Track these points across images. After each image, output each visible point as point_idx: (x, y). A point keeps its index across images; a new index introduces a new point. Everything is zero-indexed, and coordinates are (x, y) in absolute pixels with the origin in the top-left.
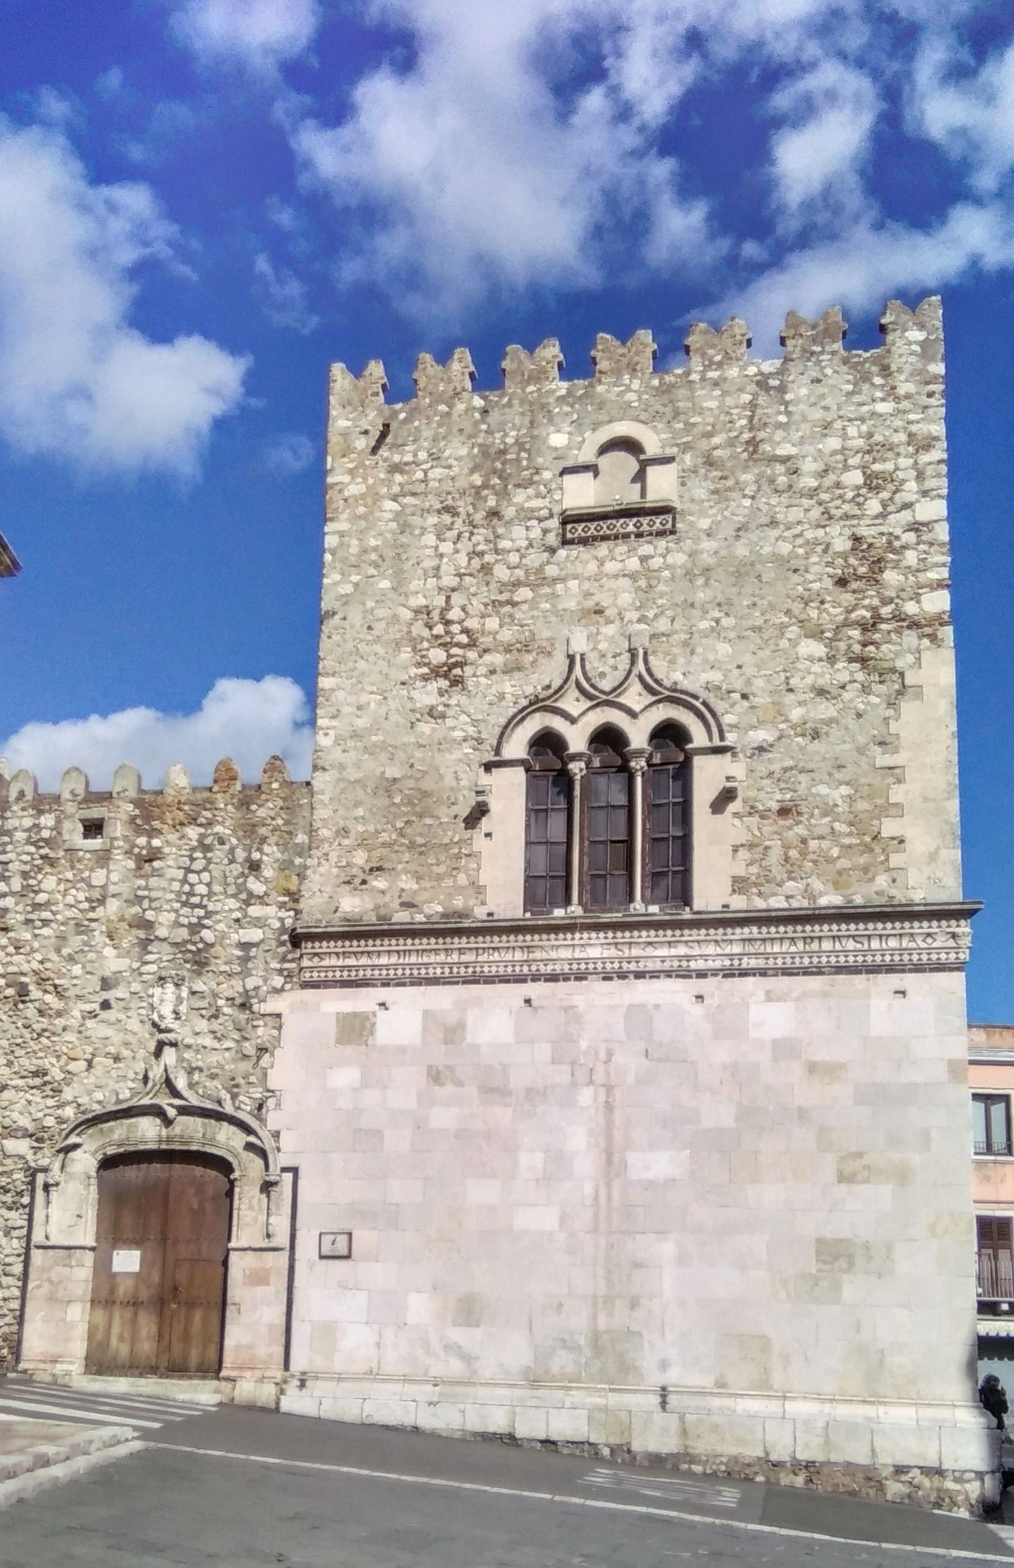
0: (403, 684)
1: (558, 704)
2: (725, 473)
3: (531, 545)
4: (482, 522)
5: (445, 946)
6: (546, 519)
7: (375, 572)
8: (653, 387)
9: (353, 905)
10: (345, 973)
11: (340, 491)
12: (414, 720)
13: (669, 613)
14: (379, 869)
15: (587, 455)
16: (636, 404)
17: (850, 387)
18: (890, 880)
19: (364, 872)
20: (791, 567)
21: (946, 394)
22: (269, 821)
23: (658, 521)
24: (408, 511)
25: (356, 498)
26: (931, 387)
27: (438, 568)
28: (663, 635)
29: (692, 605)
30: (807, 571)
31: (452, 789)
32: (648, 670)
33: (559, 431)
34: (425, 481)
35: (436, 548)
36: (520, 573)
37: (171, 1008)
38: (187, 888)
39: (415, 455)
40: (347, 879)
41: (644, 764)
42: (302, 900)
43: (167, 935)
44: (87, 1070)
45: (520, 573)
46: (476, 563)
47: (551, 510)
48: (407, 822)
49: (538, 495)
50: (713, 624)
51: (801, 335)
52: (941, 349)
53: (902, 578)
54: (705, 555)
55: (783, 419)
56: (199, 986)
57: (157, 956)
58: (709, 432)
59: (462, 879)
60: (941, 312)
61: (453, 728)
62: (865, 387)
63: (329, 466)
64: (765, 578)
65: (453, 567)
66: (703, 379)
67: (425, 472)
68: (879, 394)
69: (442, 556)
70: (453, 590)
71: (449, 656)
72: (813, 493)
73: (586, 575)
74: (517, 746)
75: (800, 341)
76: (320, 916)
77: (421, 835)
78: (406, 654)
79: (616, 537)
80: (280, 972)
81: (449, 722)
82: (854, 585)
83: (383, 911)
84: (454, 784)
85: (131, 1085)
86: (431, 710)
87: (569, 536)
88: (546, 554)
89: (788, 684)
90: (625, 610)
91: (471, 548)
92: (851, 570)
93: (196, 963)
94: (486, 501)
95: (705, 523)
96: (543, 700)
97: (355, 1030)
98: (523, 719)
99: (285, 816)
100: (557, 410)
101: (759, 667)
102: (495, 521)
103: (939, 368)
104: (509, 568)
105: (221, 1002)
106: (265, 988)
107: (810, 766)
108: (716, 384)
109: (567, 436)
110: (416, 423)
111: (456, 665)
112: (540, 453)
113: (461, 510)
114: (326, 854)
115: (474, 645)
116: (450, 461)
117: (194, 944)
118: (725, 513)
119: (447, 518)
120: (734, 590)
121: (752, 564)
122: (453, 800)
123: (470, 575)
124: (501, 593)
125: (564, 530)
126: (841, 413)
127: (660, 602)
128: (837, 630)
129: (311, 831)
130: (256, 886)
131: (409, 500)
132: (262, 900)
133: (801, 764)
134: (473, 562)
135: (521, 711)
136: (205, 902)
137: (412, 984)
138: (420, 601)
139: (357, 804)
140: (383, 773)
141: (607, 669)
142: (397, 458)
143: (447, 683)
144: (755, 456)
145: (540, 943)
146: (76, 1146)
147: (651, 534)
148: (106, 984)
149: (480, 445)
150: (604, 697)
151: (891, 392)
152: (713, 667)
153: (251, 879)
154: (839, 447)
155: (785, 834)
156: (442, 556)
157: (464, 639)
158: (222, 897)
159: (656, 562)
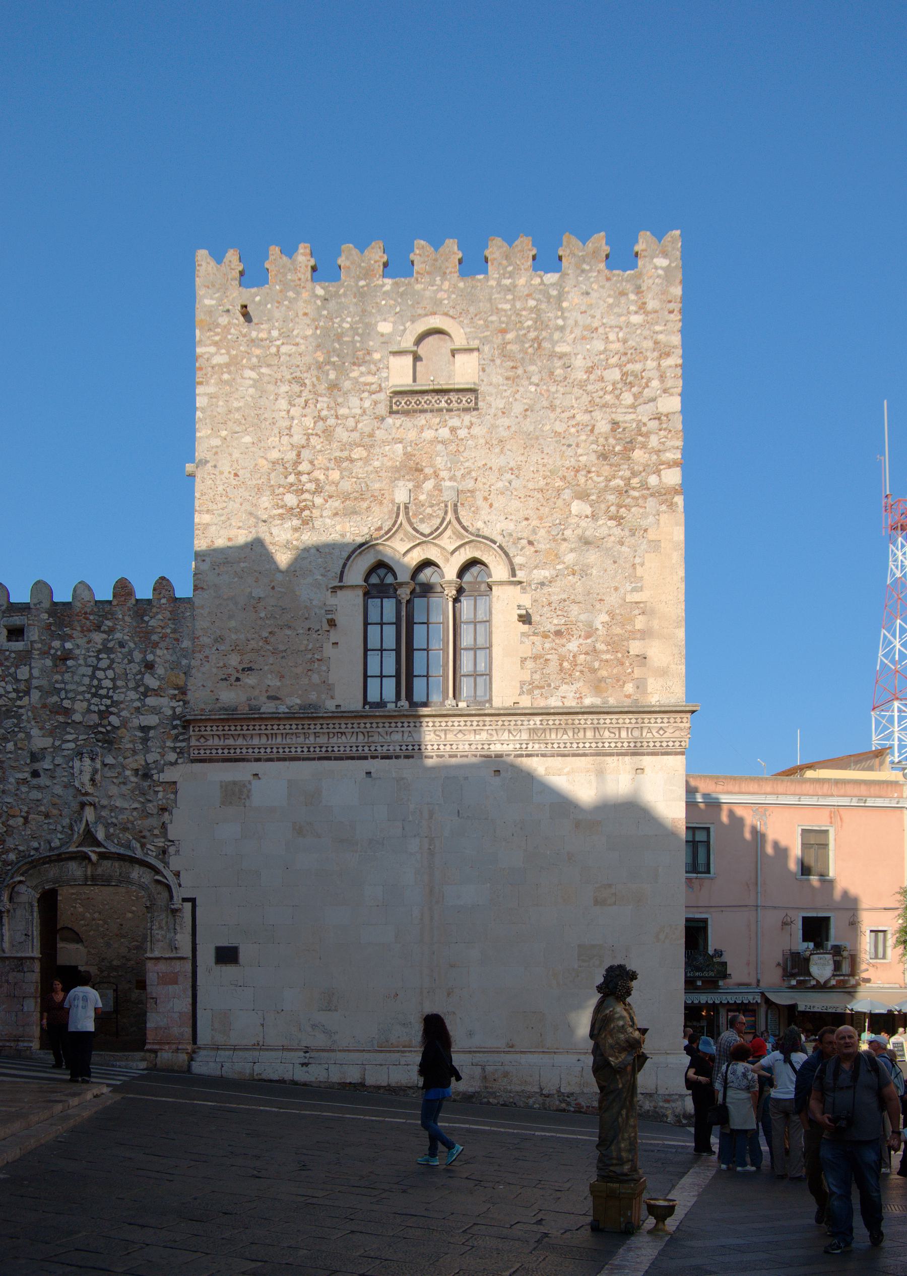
0: (265, 521)
4: (324, 392)
6: (379, 392)
7: (238, 429)
9: (229, 696)
11: (208, 360)
13: (474, 474)
14: (250, 669)
17: (611, 301)
19: (238, 671)
21: (681, 311)
22: (159, 630)
23: (464, 400)
24: (266, 379)
25: (220, 365)
26: (672, 306)
27: (290, 428)
29: (491, 468)
32: (458, 519)
33: (385, 320)
35: (288, 412)
36: (355, 435)
37: (88, 777)
38: (95, 682)
39: (270, 333)
40: (223, 677)
42: (189, 693)
43: (81, 719)
44: (25, 824)
45: (355, 435)
47: (380, 385)
48: (270, 633)
49: (369, 373)
50: (507, 484)
52: (679, 276)
55: (560, 322)
56: (110, 760)
57: (74, 736)
60: (680, 244)
62: (623, 300)
63: (197, 339)
67: (278, 348)
68: (633, 308)
69: (293, 418)
70: (303, 447)
72: (582, 385)
76: (203, 706)
78: (265, 501)
79: (432, 411)
80: (174, 749)
83: (253, 703)
85: (60, 836)
86: (287, 543)
87: (395, 408)
91: (316, 414)
93: (106, 741)
94: (328, 375)
98: (360, 553)
99: (173, 626)
100: (383, 302)
103: (677, 291)
105: (128, 773)
106: (162, 762)
108: (509, 289)
110: (269, 306)
113: (307, 381)
114: (207, 657)
116: (298, 340)
117: (104, 727)
119: (296, 388)
120: (523, 458)
123: (317, 435)
124: (342, 451)
126: (604, 321)
127: (466, 464)
129: (194, 639)
130: (151, 682)
131: (264, 370)
132: (157, 693)
136: (111, 694)
138: (274, 455)
139: (230, 617)
140: (251, 593)
142: (254, 334)
146: (20, 882)
147: (459, 410)
148: (35, 757)
150: (425, 539)
153: (147, 676)
154: (602, 348)
158: (124, 690)
159: (462, 433)
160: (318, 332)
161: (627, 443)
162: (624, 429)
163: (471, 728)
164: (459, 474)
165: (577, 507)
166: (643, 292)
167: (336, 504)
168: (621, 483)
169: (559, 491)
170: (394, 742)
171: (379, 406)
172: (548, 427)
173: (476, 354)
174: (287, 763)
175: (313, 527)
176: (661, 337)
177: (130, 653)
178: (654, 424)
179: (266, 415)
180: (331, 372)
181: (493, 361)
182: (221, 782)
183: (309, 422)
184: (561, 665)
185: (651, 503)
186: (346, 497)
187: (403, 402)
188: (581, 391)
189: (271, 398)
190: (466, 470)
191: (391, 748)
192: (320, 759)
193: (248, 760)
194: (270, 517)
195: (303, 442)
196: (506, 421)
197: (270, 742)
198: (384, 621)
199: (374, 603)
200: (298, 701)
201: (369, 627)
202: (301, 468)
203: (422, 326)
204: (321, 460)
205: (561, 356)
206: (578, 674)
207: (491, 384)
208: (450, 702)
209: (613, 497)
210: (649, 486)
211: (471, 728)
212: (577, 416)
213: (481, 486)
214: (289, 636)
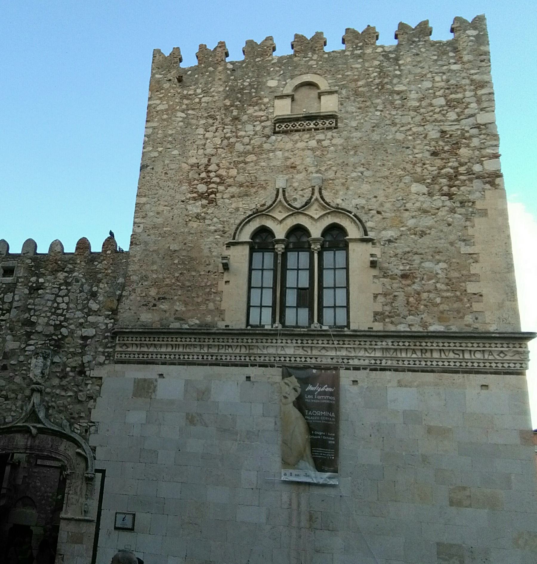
0: (183, 201)
1: (270, 214)
2: (365, 99)
3: (256, 134)
4: (229, 123)
5: (200, 343)
8: (325, 58)
10: (141, 356)
12: (188, 220)
14: (164, 298)
15: (288, 90)
16: (315, 66)
17: (436, 57)
18: (474, 318)
20: (403, 145)
28: (331, 180)
29: (347, 164)
30: (414, 148)
31: (208, 257)
32: (322, 198)
33: (272, 79)
34: (200, 103)
46: (225, 142)
47: (267, 117)
48: (181, 274)
50: (360, 174)
51: (407, 33)
53: (471, 152)
54: (354, 139)
55: (398, 73)
58: (356, 79)
59: (211, 306)
61: (209, 225)
64: (389, 151)
65: (212, 145)
66: (352, 54)
67: (200, 99)
69: (207, 139)
70: (213, 155)
71: (209, 189)
72: (416, 109)
73: (287, 149)
74: (246, 236)
75: (406, 36)
77: (189, 280)
79: (304, 130)
81: (207, 222)
82: (443, 155)
83: (165, 322)
84: (209, 255)
87: (277, 129)
88: (264, 139)
89: (405, 206)
90: (309, 166)
91: (223, 136)
94: (232, 113)
95: (354, 124)
97: (144, 389)
98: (249, 221)
100: (272, 69)
102: (237, 122)
104: (243, 145)
107: (420, 251)
108: (360, 56)
109: (277, 81)
111: (212, 193)
112: (262, 90)
113: (218, 117)
115: (223, 183)
118: (366, 118)
119: (211, 121)
121: (382, 144)
122: (208, 263)
123: (222, 148)
124: (239, 157)
125: (275, 126)
126: (431, 70)
127: (329, 163)
128: (434, 179)
133: (415, 250)
134: (224, 141)
135: (248, 217)
137: (180, 364)
138: (193, 161)
141: (298, 197)
143: (207, 202)
144: (382, 91)
145: (257, 344)
147: (323, 129)
149: (230, 86)
150: (297, 211)
151: (459, 60)
152: (359, 197)
154: (430, 86)
155: (406, 289)
156: (207, 139)
157: (218, 180)
160: (227, 88)
161: (454, 144)
162: (451, 136)
163: (333, 346)
164: (323, 169)
165: (415, 188)
166: (459, 51)
167: (233, 190)
168: (452, 171)
169: (401, 178)
170: (270, 354)
171: (266, 129)
172: (391, 137)
173: (335, 96)
174: (185, 367)
175: (216, 205)
176: (474, 77)
177: (82, 285)
178: (475, 131)
179: (189, 138)
180: (234, 110)
182: (135, 379)
183: (218, 141)
185: (477, 184)
187: (283, 126)
188: (415, 113)
189: (194, 127)
190: (329, 166)
192: (211, 365)
193: (157, 364)
194: (187, 199)
195: (213, 153)
196: (358, 134)
197: (173, 350)
198: (265, 268)
199: (257, 256)
200: (197, 322)
201: (253, 272)
202: (213, 167)
203: (298, 81)
205: (398, 93)
206: (422, 307)
208: (316, 325)
209: (444, 180)
210: (474, 172)
211: (333, 346)
212: (413, 129)
213: (340, 176)
214: (194, 276)
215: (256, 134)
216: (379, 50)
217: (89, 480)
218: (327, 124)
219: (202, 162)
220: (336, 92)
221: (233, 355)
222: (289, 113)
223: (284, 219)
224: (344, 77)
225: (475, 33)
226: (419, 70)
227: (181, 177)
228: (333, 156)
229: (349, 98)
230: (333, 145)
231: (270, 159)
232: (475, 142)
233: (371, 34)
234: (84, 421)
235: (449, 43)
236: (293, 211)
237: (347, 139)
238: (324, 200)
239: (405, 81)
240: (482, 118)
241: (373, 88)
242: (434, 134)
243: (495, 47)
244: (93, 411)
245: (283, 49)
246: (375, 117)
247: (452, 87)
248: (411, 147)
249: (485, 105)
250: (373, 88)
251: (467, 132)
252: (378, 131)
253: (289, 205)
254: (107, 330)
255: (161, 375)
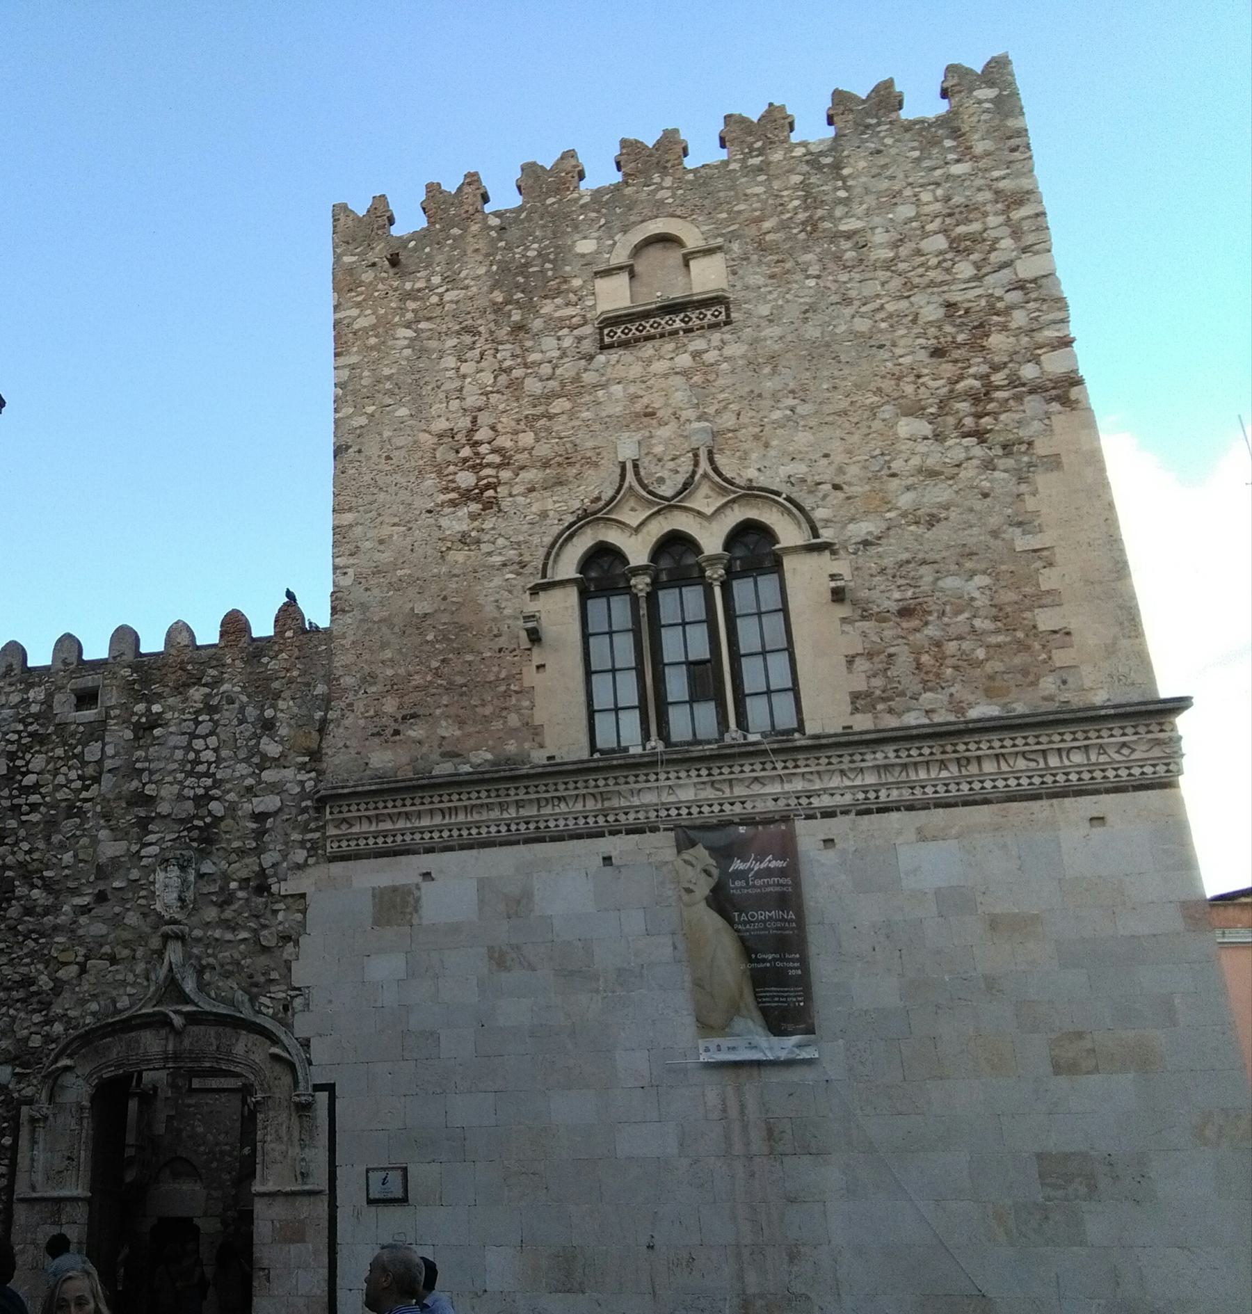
0: (430, 512)
1: (613, 517)
2: (780, 257)
3: (564, 355)
5: (499, 800)
6: (582, 325)
8: (688, 182)
10: (380, 840)
14: (414, 716)
16: (670, 200)
17: (916, 154)
18: (1059, 682)
20: (869, 343)
28: (730, 431)
29: (760, 395)
30: (894, 345)
31: (494, 619)
33: (585, 238)
34: (441, 304)
36: (553, 384)
41: (722, 572)
45: (553, 384)
46: (503, 379)
48: (443, 661)
50: (788, 412)
51: (851, 110)
53: (1012, 339)
54: (769, 342)
55: (842, 194)
59: (513, 720)
61: (490, 554)
64: (843, 358)
65: (475, 388)
67: (441, 296)
69: (464, 377)
71: (479, 479)
72: (889, 265)
73: (631, 377)
74: (567, 567)
75: (851, 117)
77: (461, 673)
79: (662, 336)
81: (485, 548)
82: (956, 354)
83: (421, 764)
87: (607, 340)
88: (583, 362)
89: (889, 468)
90: (681, 409)
91: (497, 366)
92: (950, 339)
94: (510, 316)
95: (764, 310)
96: (595, 513)
97: (395, 907)
98: (571, 537)
101: (850, 452)
102: (522, 334)
104: (541, 380)
107: (931, 556)
108: (760, 170)
111: (488, 486)
112: (565, 262)
113: (481, 329)
115: (508, 464)
118: (787, 296)
119: (468, 339)
121: (828, 345)
122: (496, 632)
123: (498, 392)
125: (601, 334)
126: (910, 180)
127: (721, 396)
128: (942, 404)
133: (920, 556)
135: (569, 528)
137: (462, 847)
138: (441, 425)
143: (480, 506)
145: (617, 788)
147: (702, 328)
149: (500, 262)
151: (966, 153)
154: (913, 214)
156: (464, 377)
157: (497, 459)
160: (494, 268)
161: (975, 328)
162: (967, 311)
163: (775, 773)
165: (906, 427)
166: (964, 134)
167: (529, 475)
168: (977, 384)
169: (873, 410)
170: (646, 805)
171: (584, 342)
172: (843, 328)
173: (718, 258)
174: (474, 852)
175: (500, 510)
176: (1002, 185)
177: (242, 709)
178: (1016, 296)
179: (427, 379)
181: (747, 259)
182: (374, 889)
184: (917, 661)
185: (1033, 404)
186: (546, 464)
188: (889, 274)
191: (641, 815)
192: (528, 841)
193: (415, 852)
194: (437, 505)
196: (776, 331)
197: (446, 821)
198: (614, 628)
199: (597, 607)
200: (489, 756)
201: (592, 640)
202: (483, 434)
203: (637, 236)
204: (506, 422)
205: (848, 236)
206: (949, 671)
207: (747, 288)
209: (964, 404)
210: (1024, 380)
211: (775, 773)
213: (747, 421)
214: (470, 663)
215: (564, 355)
216: (799, 152)
217: (304, 1109)
218: (709, 316)
219: (460, 425)
220: (720, 248)
221: (570, 816)
222: (627, 303)
223: (643, 524)
224: (733, 216)
225: (991, 93)
226: (885, 184)
227: (421, 462)
228: (729, 381)
229: (747, 259)
230: (727, 359)
231: (600, 403)
232: (1019, 318)
233: (778, 120)
234: (278, 988)
235: (941, 121)
236: (659, 504)
237: (754, 342)
238: (720, 475)
239: (860, 210)
240: (1027, 268)
241: (795, 231)
242: (932, 312)
243: (1037, 118)
244: (294, 964)
245: (601, 173)
246: (806, 291)
247: (958, 210)
248: (888, 343)
249: (1030, 239)
250: (795, 231)
251: (1000, 299)
252: (816, 319)
253: (650, 492)
254: (303, 795)
255: (427, 875)
